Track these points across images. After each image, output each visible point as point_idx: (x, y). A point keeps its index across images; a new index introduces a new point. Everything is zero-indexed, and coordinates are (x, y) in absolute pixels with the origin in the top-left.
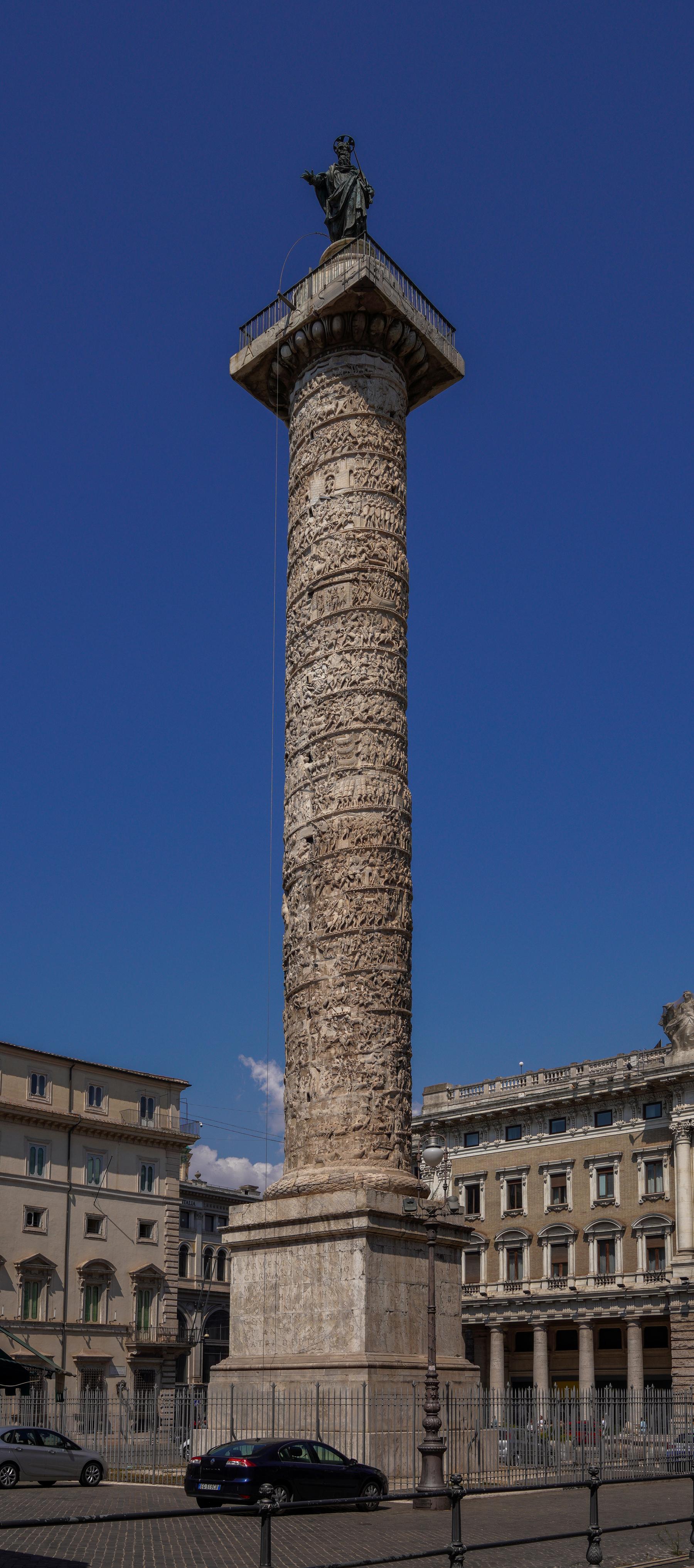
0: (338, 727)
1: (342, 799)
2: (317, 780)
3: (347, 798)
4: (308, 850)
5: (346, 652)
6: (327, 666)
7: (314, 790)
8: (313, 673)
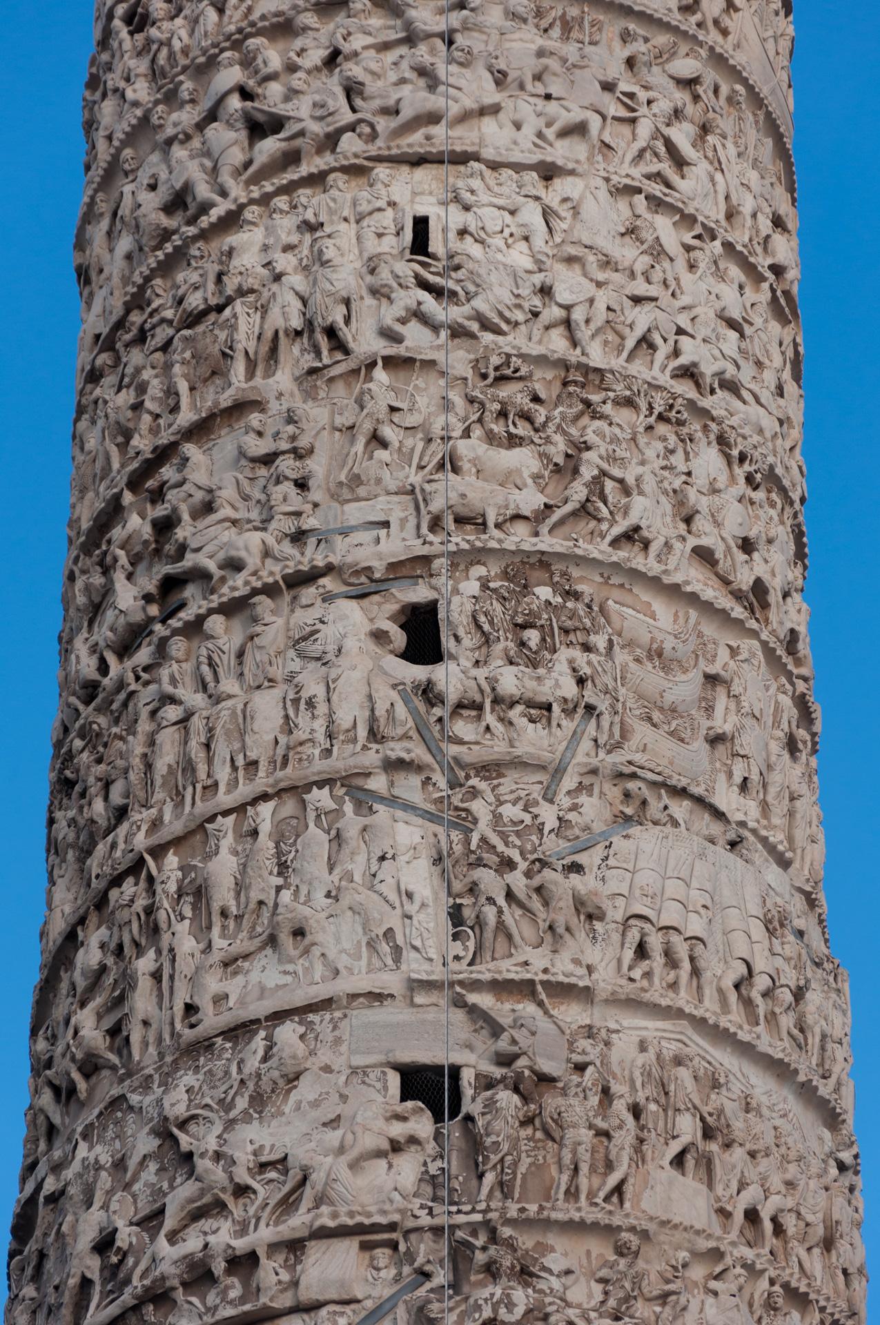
0: (615, 543)
1: (655, 942)
2: (491, 770)
3: (682, 950)
4: (413, 1140)
5: (656, 204)
6: (547, 213)
7: (464, 821)
8: (457, 218)
